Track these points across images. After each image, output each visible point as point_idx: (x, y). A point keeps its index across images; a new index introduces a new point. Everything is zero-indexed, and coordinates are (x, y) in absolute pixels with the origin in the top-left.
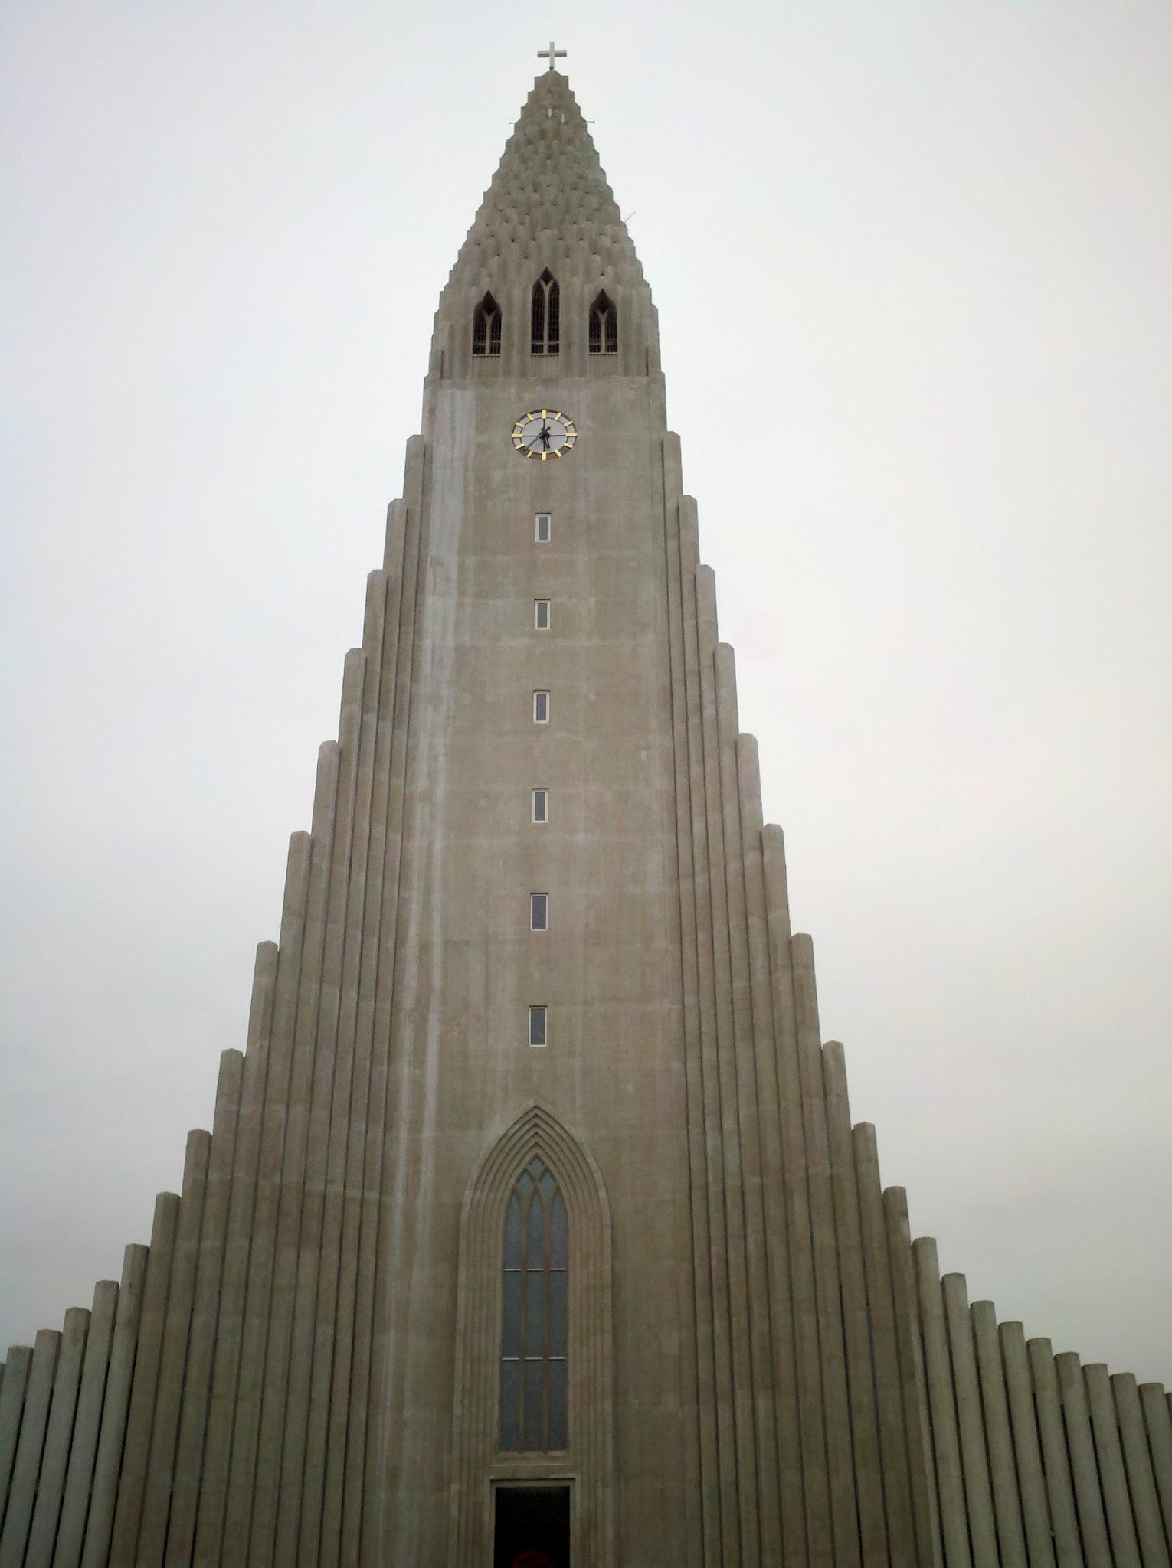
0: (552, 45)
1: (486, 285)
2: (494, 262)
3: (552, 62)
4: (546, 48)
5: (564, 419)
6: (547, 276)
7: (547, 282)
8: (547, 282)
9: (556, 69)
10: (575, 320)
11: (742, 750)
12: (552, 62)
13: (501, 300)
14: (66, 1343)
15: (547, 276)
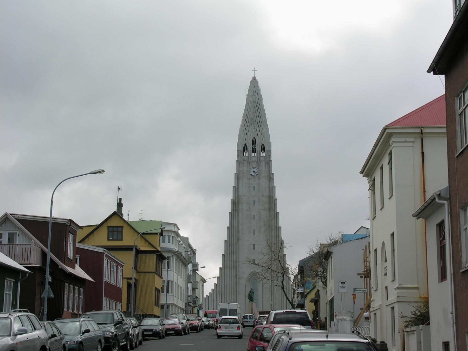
0: (254, 68)
1: (245, 142)
2: (246, 136)
3: (254, 72)
4: (253, 70)
5: (257, 169)
6: (254, 138)
7: (254, 139)
8: (254, 139)
9: (255, 76)
10: (258, 148)
11: (280, 228)
12: (254, 72)
13: (247, 145)
14: (207, 299)
15: (254, 138)
